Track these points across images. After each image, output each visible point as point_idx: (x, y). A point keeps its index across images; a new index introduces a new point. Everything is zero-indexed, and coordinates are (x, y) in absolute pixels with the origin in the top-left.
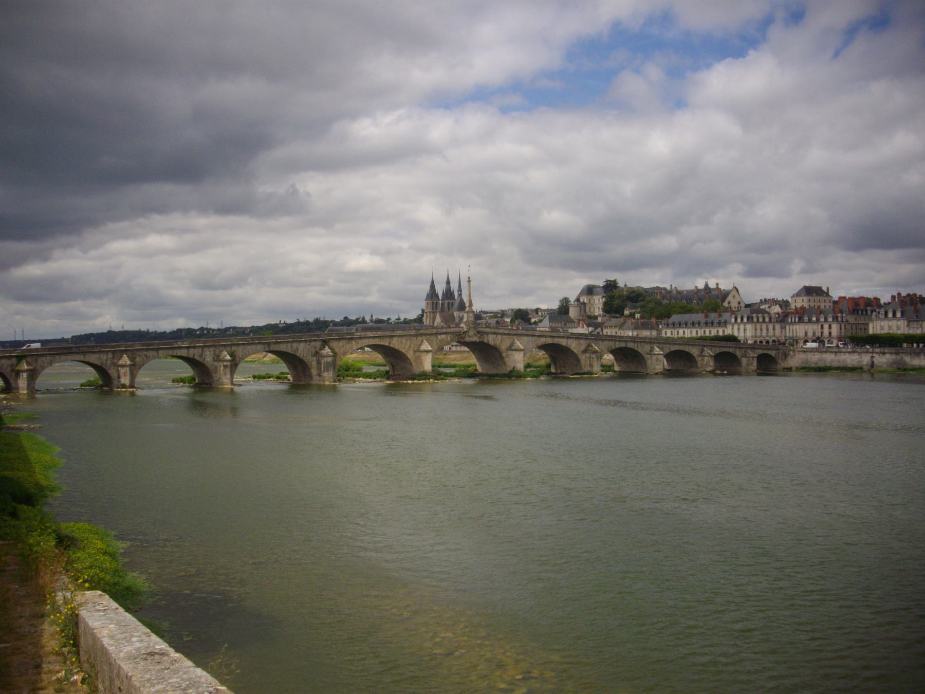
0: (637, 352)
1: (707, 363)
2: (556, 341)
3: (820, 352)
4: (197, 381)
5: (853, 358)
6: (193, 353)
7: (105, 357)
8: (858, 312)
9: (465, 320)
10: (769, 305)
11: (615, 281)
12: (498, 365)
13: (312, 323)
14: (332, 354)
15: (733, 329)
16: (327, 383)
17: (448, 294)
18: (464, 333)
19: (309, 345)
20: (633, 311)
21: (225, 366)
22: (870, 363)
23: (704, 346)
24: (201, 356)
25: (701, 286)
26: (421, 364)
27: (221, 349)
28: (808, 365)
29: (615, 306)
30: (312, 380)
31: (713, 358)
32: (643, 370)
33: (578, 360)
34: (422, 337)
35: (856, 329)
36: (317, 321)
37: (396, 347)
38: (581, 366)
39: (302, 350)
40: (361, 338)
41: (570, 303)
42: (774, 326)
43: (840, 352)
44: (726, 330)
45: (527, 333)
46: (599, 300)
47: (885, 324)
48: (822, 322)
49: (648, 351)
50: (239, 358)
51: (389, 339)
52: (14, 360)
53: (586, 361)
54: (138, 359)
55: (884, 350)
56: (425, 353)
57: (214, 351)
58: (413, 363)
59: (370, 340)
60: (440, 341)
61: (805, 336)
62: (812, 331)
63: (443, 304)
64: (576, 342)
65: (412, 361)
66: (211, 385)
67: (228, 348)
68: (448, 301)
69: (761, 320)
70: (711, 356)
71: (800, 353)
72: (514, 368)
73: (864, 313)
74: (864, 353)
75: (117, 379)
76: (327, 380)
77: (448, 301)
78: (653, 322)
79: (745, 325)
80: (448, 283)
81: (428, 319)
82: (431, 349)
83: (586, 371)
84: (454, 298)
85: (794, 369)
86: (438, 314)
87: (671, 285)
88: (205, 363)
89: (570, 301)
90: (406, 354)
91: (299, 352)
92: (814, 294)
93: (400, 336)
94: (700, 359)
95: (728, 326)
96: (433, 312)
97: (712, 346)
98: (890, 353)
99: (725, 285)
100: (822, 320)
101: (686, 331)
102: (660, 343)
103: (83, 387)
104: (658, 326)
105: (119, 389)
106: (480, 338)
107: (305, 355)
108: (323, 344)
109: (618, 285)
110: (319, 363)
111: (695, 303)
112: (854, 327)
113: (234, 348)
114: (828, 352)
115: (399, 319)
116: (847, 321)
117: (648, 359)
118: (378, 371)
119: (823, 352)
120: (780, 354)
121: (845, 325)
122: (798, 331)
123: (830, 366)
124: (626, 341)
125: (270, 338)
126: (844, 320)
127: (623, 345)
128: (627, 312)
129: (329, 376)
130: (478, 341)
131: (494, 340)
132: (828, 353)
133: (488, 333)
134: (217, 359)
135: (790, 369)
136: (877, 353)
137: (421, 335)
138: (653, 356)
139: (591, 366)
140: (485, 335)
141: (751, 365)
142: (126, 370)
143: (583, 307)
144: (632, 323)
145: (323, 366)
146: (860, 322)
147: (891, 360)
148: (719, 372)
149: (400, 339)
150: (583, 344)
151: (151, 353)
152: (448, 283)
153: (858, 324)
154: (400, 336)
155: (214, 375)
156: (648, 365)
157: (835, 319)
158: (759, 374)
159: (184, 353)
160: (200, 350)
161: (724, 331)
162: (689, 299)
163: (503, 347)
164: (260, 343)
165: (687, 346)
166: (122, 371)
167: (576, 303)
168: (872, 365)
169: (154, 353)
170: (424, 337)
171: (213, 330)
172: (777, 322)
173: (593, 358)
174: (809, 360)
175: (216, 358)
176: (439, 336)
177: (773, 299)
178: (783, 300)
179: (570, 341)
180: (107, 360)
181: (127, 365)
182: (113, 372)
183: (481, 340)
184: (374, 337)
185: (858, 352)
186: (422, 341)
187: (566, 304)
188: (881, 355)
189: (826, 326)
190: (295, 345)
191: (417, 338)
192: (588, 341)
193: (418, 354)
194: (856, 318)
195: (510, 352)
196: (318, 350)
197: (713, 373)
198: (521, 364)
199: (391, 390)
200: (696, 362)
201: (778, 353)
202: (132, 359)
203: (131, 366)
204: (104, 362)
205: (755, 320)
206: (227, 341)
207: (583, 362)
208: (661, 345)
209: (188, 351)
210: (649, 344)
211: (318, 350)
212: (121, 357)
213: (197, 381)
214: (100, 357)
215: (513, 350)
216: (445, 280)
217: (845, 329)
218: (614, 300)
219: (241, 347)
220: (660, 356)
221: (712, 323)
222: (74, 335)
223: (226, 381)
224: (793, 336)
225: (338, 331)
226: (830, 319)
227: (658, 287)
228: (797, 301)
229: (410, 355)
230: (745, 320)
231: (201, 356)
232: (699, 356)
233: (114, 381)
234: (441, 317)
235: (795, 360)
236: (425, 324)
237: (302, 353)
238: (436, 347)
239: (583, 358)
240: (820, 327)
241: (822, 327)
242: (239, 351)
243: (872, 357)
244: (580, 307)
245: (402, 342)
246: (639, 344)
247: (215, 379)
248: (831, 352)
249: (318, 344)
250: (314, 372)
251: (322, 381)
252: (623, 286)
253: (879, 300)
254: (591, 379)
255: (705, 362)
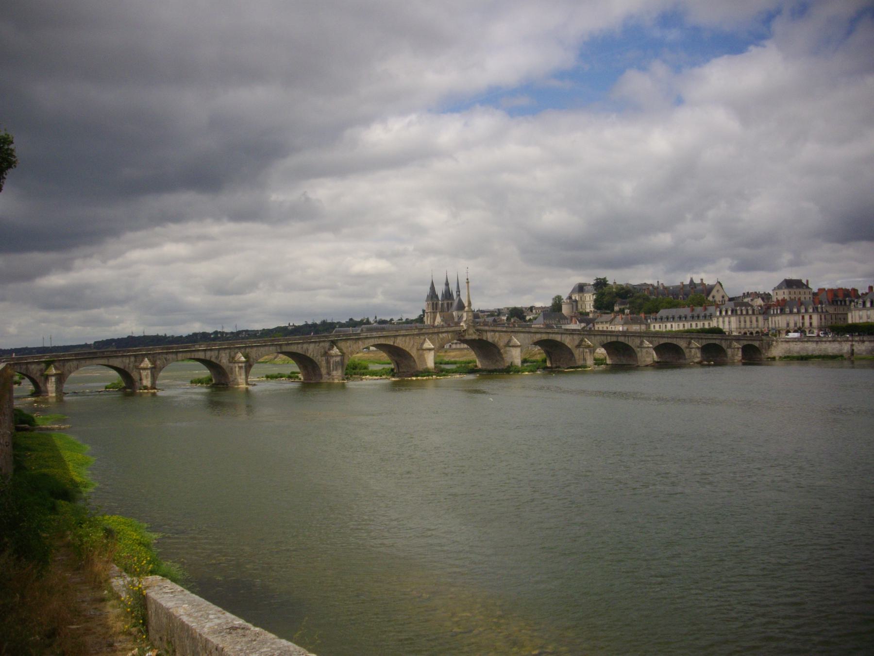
0: (628, 345)
1: (694, 354)
2: (552, 337)
3: (802, 342)
4: (214, 381)
5: (834, 346)
6: (211, 356)
7: (127, 361)
8: (837, 303)
9: (464, 319)
10: (751, 298)
11: (605, 278)
12: (497, 361)
13: (319, 325)
14: (340, 353)
15: (718, 322)
16: (336, 381)
17: (448, 295)
18: (463, 331)
19: (318, 346)
20: (623, 307)
21: (240, 368)
22: (850, 351)
23: (692, 339)
24: (217, 358)
25: (687, 282)
26: (424, 360)
27: (236, 351)
28: (790, 355)
29: (605, 302)
30: (322, 378)
31: (700, 349)
32: (634, 363)
33: (571, 354)
34: (424, 336)
35: (836, 319)
36: (324, 323)
37: (401, 346)
38: (575, 360)
39: (312, 350)
40: (367, 338)
41: (562, 301)
42: (757, 318)
43: (821, 341)
44: (711, 322)
45: (524, 330)
46: (590, 297)
47: (863, 313)
48: (803, 313)
49: (638, 344)
50: (253, 359)
51: (393, 339)
52: (43, 366)
53: (579, 355)
54: (158, 362)
55: (863, 338)
56: (428, 351)
57: (230, 353)
58: (417, 361)
59: (375, 340)
60: (442, 339)
61: (787, 327)
62: (793, 321)
63: (442, 304)
65: (415, 358)
66: (227, 385)
67: (243, 350)
68: (447, 302)
69: (744, 312)
70: (698, 348)
71: (783, 343)
72: (512, 363)
73: (843, 303)
74: (844, 341)
75: (139, 381)
76: (337, 378)
77: (447, 302)
78: (642, 317)
79: (729, 318)
80: (447, 284)
81: (429, 319)
82: (433, 347)
83: (580, 365)
84: (453, 299)
85: (777, 358)
86: (438, 315)
87: (658, 282)
88: (221, 364)
89: (562, 299)
90: (410, 352)
91: (310, 352)
92: (794, 287)
93: (403, 335)
94: (688, 350)
95: (713, 319)
96: (434, 312)
97: (698, 338)
98: (870, 341)
99: (709, 281)
100: (803, 311)
101: (674, 324)
102: (649, 337)
103: (107, 390)
104: (647, 320)
105: (141, 391)
106: (479, 335)
107: (315, 355)
108: (332, 344)
109: (607, 283)
110: (328, 362)
111: (681, 298)
112: (834, 317)
113: (248, 350)
114: (810, 341)
115: (401, 319)
116: (827, 311)
117: (639, 352)
118: (383, 369)
119: (805, 341)
120: (764, 344)
121: (825, 316)
122: (780, 322)
123: (812, 355)
124: (618, 336)
125: (282, 340)
126: (824, 310)
127: (614, 339)
128: (616, 308)
129: (338, 374)
130: (477, 338)
131: (492, 338)
132: (809, 343)
133: (486, 331)
134: (232, 360)
135: (774, 359)
136: (856, 341)
137: (423, 334)
138: (643, 349)
139: (585, 359)
140: (484, 334)
141: (737, 355)
142: (148, 373)
143: (574, 304)
144: (622, 318)
145: (332, 365)
146: (839, 312)
147: (870, 348)
148: (706, 363)
149: (404, 338)
150: (577, 339)
151: (170, 357)
152: (447, 284)
153: (838, 314)
154: (403, 335)
155: (230, 376)
156: (638, 358)
157: (815, 310)
158: (744, 364)
159: (201, 355)
160: (216, 352)
161: (709, 323)
162: (675, 295)
163: (501, 344)
164: (272, 345)
165: (675, 339)
166: (144, 373)
167: (568, 301)
168: (852, 352)
169: (174, 356)
170: (426, 336)
171: (227, 334)
172: (760, 314)
173: (587, 352)
174: (791, 349)
175: (231, 359)
176: (440, 335)
177: (756, 292)
178: (765, 293)
179: (564, 337)
180: (129, 364)
181: (149, 367)
182: (135, 375)
183: (480, 337)
184: (380, 337)
185: (838, 341)
186: (425, 340)
187: (559, 302)
188: (860, 343)
189: (807, 317)
190: (305, 346)
191: (419, 337)
192: (581, 337)
193: (421, 352)
194: (835, 309)
195: (508, 348)
196: (327, 350)
197: (700, 364)
198: (518, 359)
199: (396, 387)
200: (684, 354)
201: (762, 343)
202: (153, 362)
203: (151, 368)
204: (127, 366)
205: (739, 312)
206: (242, 343)
207: (577, 356)
208: (651, 339)
209: (205, 353)
210: (639, 338)
211: (327, 350)
212: (142, 361)
213: (214, 381)
214: (123, 361)
215: (510, 347)
216: (445, 281)
217: (825, 318)
218: (604, 297)
219: (255, 349)
220: (650, 349)
221: (698, 317)
222: (96, 341)
223: (242, 381)
224: (776, 327)
225: (344, 331)
226: (811, 310)
227: (645, 283)
228: (778, 294)
229: (414, 353)
230: (729, 313)
231: (217, 358)
232: (687, 348)
233: (137, 384)
234: (441, 317)
235: (778, 350)
236: (426, 323)
237: (312, 354)
238: (437, 345)
239: (576, 352)
240: (801, 317)
241: (803, 318)
242: (253, 353)
243: (852, 345)
244: (572, 304)
245: (405, 341)
246: (629, 338)
247: (231, 379)
248: (812, 341)
249: (327, 345)
250: (324, 371)
251: (331, 379)
252: (612, 284)
253: (857, 290)
254: (584, 372)
255: (693, 354)
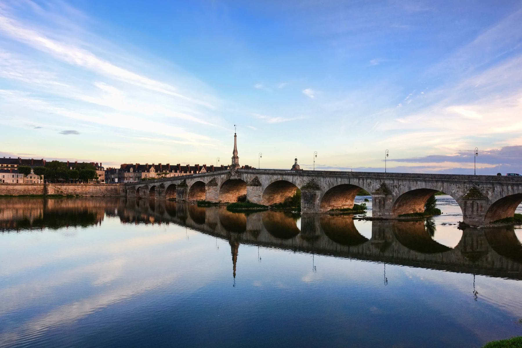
64: (300, 179)
130: (238, 179)
131: (246, 178)
165: (440, 184)
179: (296, 178)
183: (240, 178)
